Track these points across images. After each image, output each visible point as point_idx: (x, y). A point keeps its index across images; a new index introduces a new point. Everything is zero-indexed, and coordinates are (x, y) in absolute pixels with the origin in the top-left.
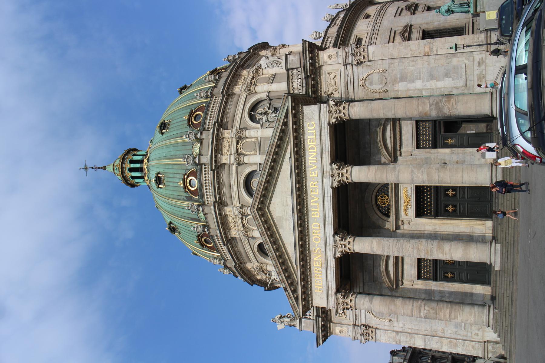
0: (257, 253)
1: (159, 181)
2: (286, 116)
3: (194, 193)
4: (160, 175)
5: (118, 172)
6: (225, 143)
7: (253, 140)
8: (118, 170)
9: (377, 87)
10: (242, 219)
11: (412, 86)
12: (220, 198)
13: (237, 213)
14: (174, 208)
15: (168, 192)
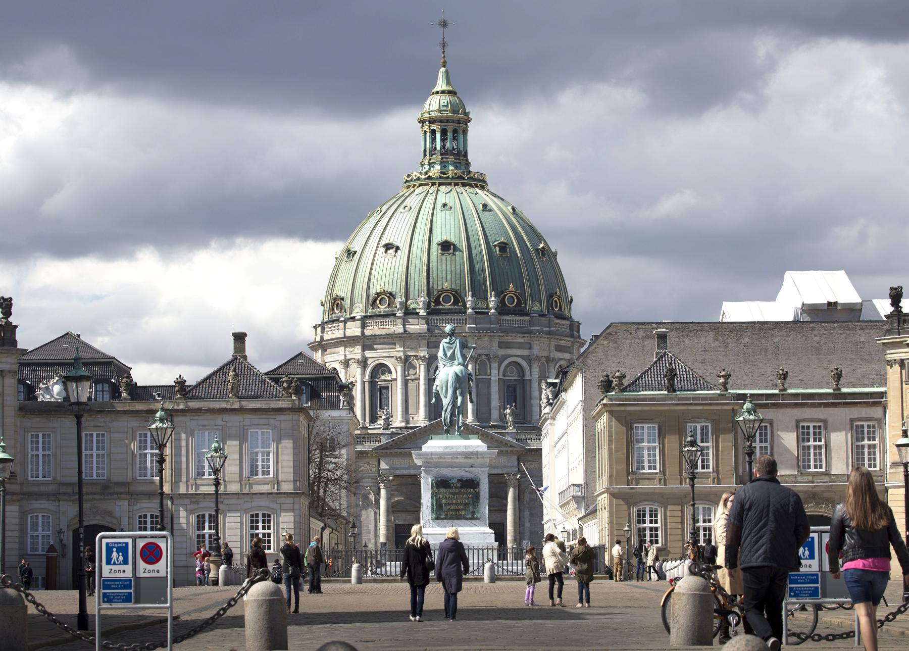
0: (377, 362)
1: (446, 246)
2: (511, 446)
3: (437, 302)
4: (452, 247)
5: (442, 109)
6: (486, 342)
7: (489, 371)
8: (445, 108)
9: (527, 497)
10: (416, 356)
11: (527, 520)
12: (436, 336)
13: (422, 354)
14: (418, 266)
15: (435, 258)
